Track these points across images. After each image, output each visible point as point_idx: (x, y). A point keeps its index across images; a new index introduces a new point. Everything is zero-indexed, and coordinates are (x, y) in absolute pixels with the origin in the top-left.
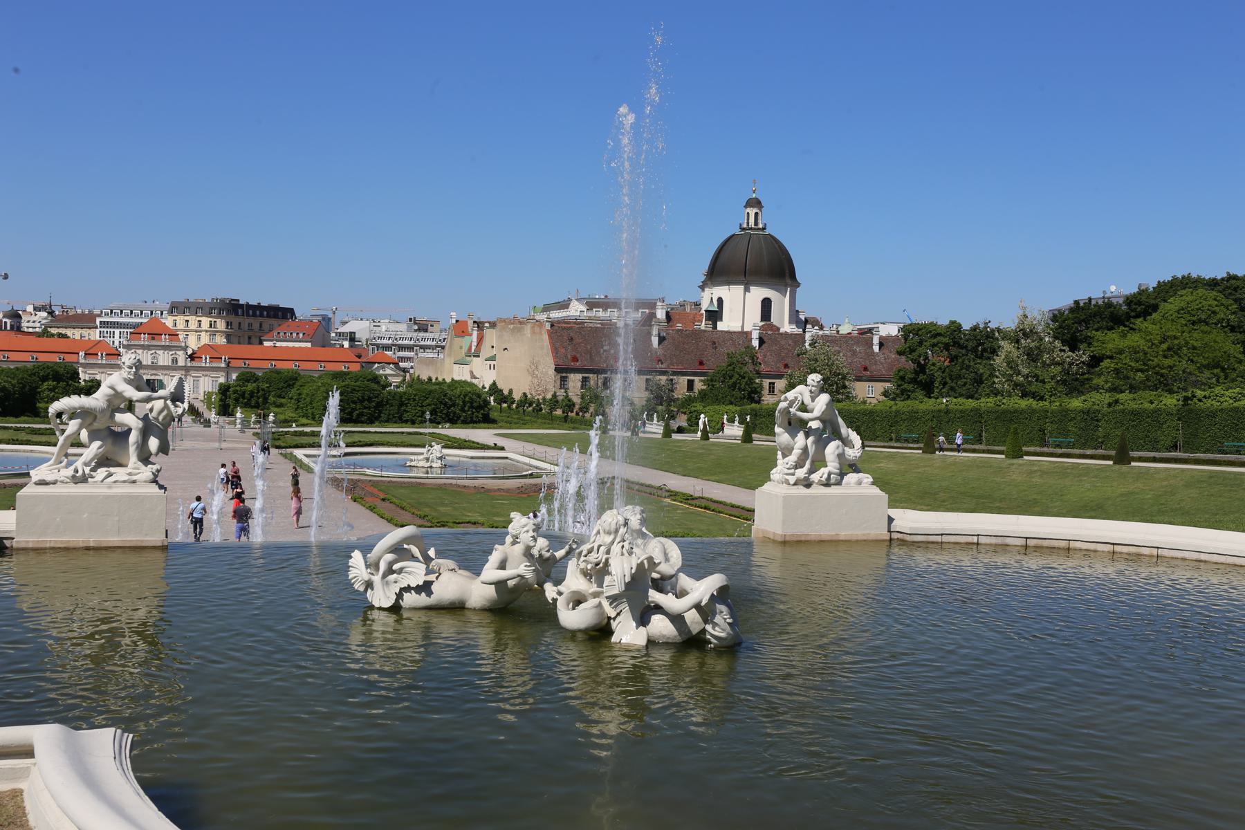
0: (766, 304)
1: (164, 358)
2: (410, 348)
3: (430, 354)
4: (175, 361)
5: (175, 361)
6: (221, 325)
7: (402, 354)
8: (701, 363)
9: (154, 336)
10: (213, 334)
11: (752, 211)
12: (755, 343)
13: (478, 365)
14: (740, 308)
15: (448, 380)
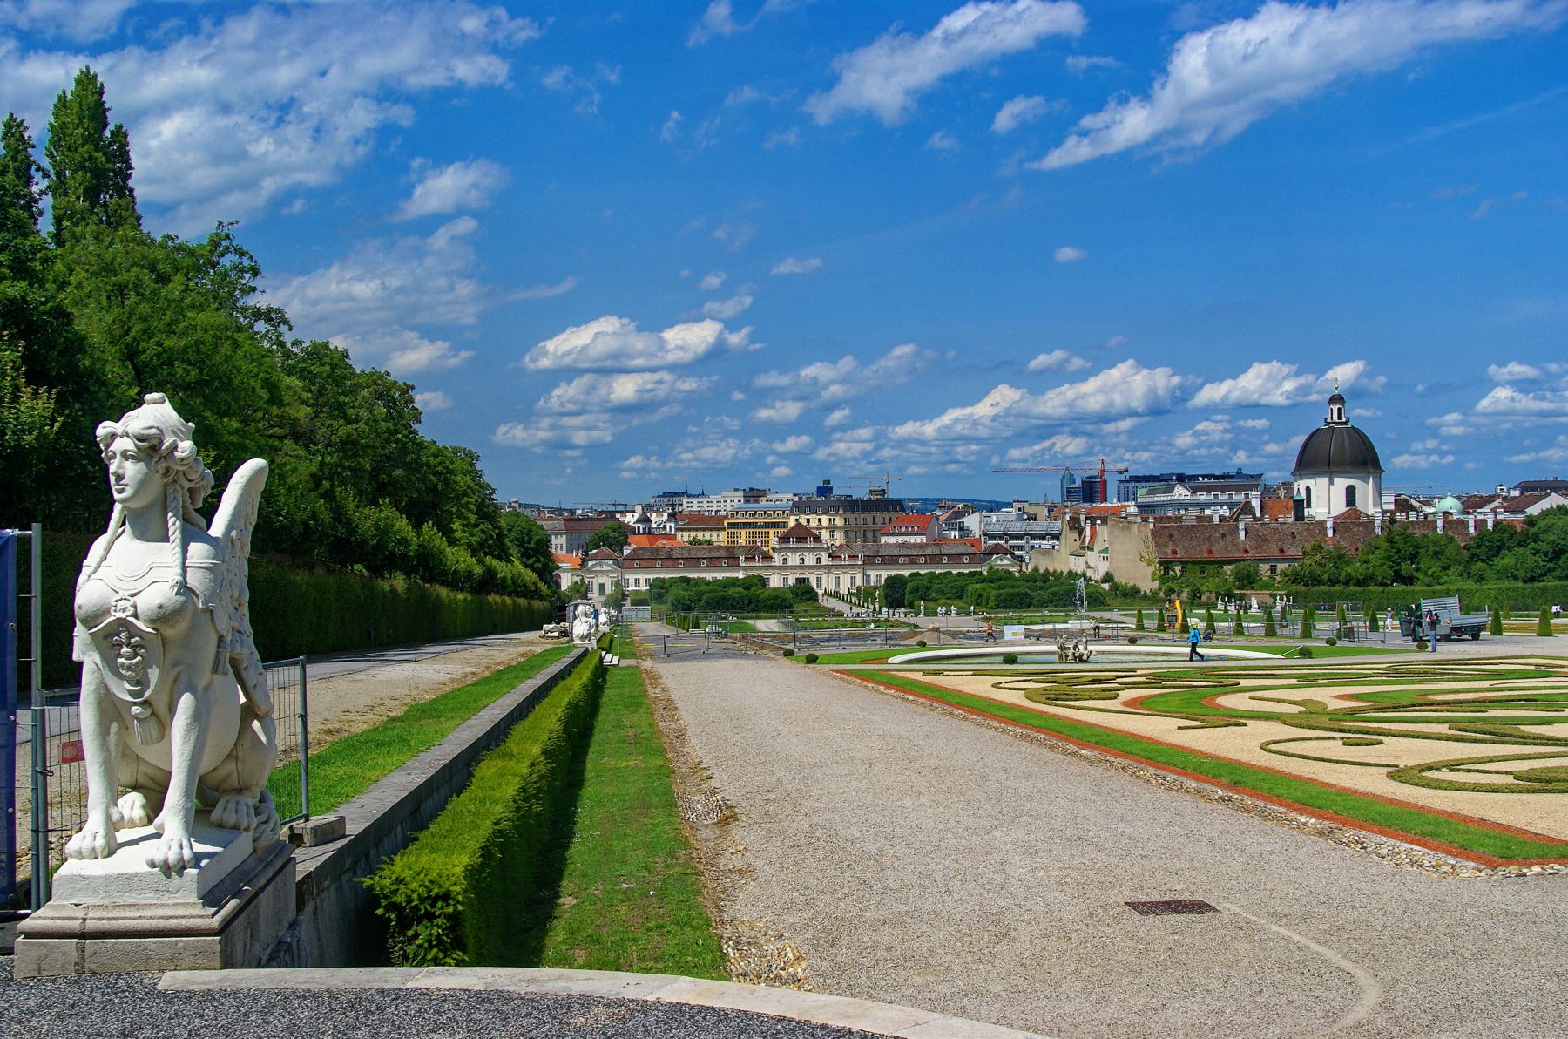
0: (1351, 491)
1: (810, 559)
2: (1021, 537)
3: (1046, 544)
4: (819, 560)
5: (819, 560)
6: (840, 522)
7: (1012, 542)
8: (1282, 551)
9: (801, 539)
10: (832, 530)
11: (1335, 408)
12: (1330, 533)
13: (1093, 557)
14: (1326, 498)
15: (1065, 572)
